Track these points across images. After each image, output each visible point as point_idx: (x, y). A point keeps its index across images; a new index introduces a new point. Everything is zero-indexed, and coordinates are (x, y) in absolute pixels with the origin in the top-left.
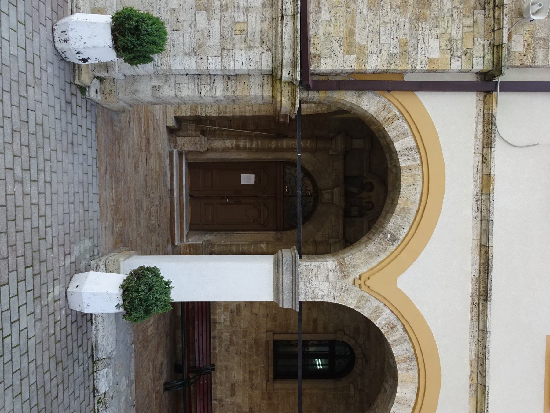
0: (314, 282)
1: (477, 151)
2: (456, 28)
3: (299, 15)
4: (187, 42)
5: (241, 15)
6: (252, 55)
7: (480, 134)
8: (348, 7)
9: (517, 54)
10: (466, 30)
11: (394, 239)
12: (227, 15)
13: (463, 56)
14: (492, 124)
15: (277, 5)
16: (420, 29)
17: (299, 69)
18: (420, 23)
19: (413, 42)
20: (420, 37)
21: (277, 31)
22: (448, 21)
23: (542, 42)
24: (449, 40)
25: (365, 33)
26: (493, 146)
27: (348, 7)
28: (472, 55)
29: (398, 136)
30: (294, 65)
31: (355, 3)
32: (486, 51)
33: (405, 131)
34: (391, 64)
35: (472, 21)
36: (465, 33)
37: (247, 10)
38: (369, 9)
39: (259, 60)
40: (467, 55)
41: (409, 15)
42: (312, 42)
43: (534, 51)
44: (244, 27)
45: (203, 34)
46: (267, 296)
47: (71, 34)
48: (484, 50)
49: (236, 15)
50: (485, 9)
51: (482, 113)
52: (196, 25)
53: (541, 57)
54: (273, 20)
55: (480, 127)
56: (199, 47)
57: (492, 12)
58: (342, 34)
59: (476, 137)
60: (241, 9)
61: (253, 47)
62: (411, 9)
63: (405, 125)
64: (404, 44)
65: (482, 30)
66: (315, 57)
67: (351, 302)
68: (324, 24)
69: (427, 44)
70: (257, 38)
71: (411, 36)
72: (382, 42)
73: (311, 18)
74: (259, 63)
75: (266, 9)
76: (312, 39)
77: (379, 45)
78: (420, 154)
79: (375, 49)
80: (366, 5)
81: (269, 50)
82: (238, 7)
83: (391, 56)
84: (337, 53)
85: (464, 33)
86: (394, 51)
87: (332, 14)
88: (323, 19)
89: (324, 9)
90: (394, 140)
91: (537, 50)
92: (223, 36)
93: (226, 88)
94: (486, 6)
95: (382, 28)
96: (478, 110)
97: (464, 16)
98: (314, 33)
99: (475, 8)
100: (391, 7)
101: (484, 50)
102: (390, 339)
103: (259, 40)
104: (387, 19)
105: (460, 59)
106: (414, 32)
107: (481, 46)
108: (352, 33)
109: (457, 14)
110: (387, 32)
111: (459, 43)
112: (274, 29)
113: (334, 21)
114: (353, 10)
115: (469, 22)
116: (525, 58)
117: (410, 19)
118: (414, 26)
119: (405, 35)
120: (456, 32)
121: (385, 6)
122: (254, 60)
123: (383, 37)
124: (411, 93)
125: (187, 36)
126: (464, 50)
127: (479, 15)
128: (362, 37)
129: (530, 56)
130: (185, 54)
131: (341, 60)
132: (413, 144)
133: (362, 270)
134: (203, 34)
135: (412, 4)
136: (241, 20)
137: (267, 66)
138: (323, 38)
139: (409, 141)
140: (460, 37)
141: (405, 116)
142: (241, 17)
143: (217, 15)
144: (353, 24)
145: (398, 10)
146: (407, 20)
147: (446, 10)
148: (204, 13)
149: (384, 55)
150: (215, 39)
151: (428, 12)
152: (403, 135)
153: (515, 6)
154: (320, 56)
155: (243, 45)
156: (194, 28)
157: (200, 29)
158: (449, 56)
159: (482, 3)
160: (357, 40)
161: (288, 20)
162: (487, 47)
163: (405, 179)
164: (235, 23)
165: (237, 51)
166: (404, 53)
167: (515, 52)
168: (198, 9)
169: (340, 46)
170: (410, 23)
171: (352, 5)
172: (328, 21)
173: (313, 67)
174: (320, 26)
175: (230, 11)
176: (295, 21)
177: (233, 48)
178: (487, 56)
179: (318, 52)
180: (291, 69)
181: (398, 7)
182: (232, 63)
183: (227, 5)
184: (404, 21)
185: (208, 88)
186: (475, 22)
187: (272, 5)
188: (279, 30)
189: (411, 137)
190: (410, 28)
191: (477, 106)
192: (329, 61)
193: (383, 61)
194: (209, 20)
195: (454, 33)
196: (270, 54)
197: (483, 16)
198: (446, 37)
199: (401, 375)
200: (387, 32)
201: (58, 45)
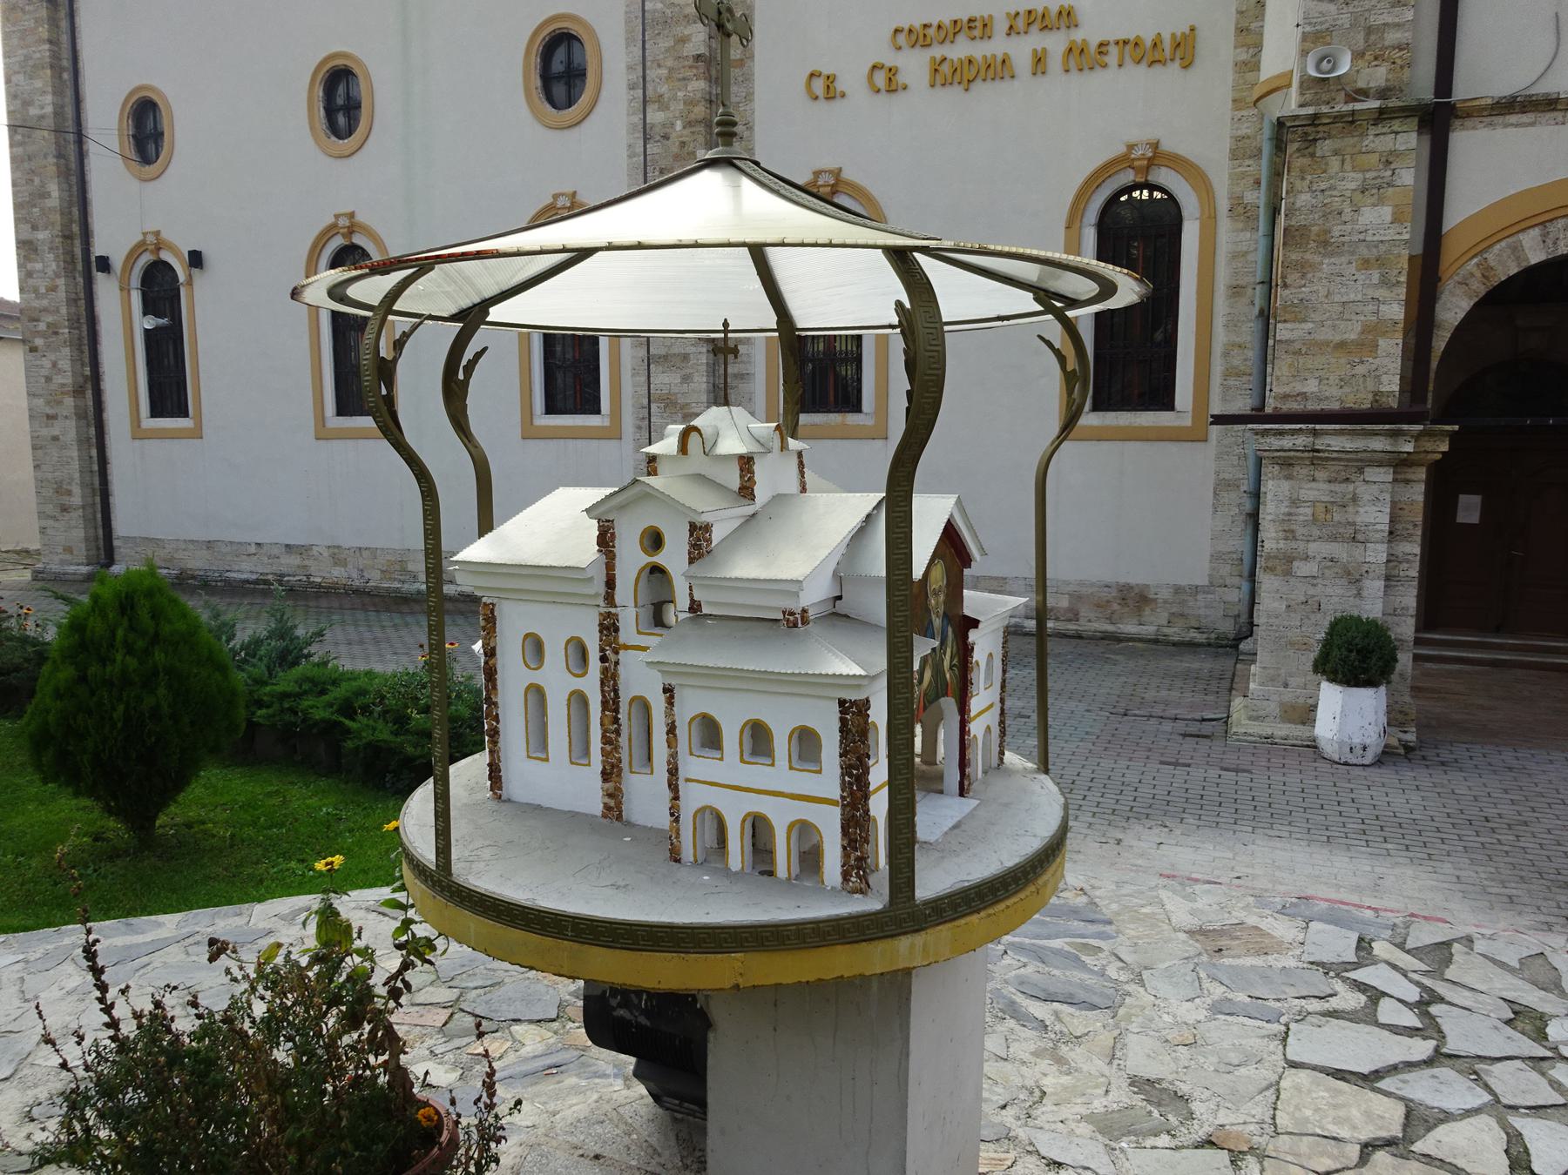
1: (1560, 119)
2: (1343, 183)
3: (1318, 427)
4: (1340, 591)
5: (1301, 510)
6: (1367, 497)
7: (1526, 118)
8: (1299, 353)
9: (1390, 76)
10: (1348, 166)
12: (1300, 531)
13: (1393, 166)
14: (1515, 101)
15: (1289, 458)
16: (1342, 239)
17: (1405, 427)
18: (1333, 240)
19: (1363, 251)
20: (1355, 238)
21: (1334, 459)
22: (1331, 196)
23: (1373, 37)
24: (1363, 192)
25: (1342, 325)
26: (1555, 96)
27: (1299, 353)
28: (1391, 152)
29: (1518, 258)
31: (1293, 341)
32: (1384, 130)
33: (1509, 246)
34: (1398, 282)
35: (1334, 158)
36: (1353, 167)
37: (1295, 502)
38: (1304, 321)
39: (1376, 486)
40: (1390, 160)
41: (1317, 259)
42: (1352, 405)
43: (1386, 48)
44: (1320, 508)
45: (1327, 568)
47: (1357, 740)
48: (1384, 134)
49: (1301, 518)
50: (1315, 140)
51: (1488, 120)
52: (1314, 577)
53: (1398, 35)
54: (1313, 464)
55: (1513, 119)
56: (1349, 574)
57: (1320, 128)
58: (1343, 361)
59: (1532, 124)
60: (1292, 511)
61: (1355, 494)
62: (1308, 256)
63: (1498, 246)
64: (1366, 264)
65: (1350, 141)
66: (1377, 401)
68: (1325, 388)
69: (1368, 227)
71: (1353, 253)
72: (1359, 297)
73: (1312, 406)
74: (1382, 486)
75: (1295, 474)
76: (1348, 405)
77: (1364, 302)
78: (1556, 218)
79: (1371, 308)
80: (1297, 325)
81: (1361, 470)
82: (1290, 514)
83: (1385, 282)
84: (1374, 367)
85: (1354, 169)
86: (1376, 276)
87: (1307, 374)
88: (1316, 390)
89: (1299, 387)
90: (1524, 265)
91: (1387, 43)
92: (1334, 538)
93: (1408, 538)
94: (1311, 138)
95: (1337, 298)
96: (1482, 125)
97: (1325, 172)
98: (1338, 403)
99: (1313, 155)
100: (1304, 286)
101: (1384, 134)
103: (1344, 485)
104: (1323, 292)
105: (1397, 172)
106: (1346, 248)
107: (1377, 140)
108: (1342, 345)
109: (1320, 184)
110: (1342, 290)
111: (1368, 175)
112: (1329, 463)
113: (1321, 373)
114: (1304, 344)
115: (1335, 163)
116: (1399, 62)
117: (1324, 256)
118: (1336, 250)
119: (1350, 263)
120: (1352, 181)
121: (1301, 296)
122: (1376, 494)
123: (1352, 297)
124: (1444, 241)
125: (1329, 591)
126: (1381, 167)
127: (1324, 147)
128: (1350, 328)
129: (1396, 54)
130: (1359, 595)
131: (1386, 361)
132: (1536, 232)
134: (1327, 568)
135: (1301, 255)
136: (1309, 511)
137: (1384, 475)
138: (1347, 389)
140: (1360, 175)
141: (1481, 248)
142: (1305, 512)
143: (1301, 546)
144: (1327, 343)
145: (1310, 276)
146: (1326, 261)
147: (1314, 201)
148: (1296, 564)
149: (1381, 293)
150: (1339, 550)
151: (1315, 229)
152: (1516, 250)
153: (1309, 89)
154: (1376, 394)
155: (1350, 509)
156: (1319, 581)
157: (1320, 572)
158: (1390, 189)
159: (1307, 144)
160: (1353, 336)
161: (1320, 443)
162: (1379, 129)
164: (1315, 519)
165: (1359, 520)
166: (1380, 262)
167: (1387, 80)
168: (1288, 573)
169: (1362, 362)
170: (1332, 255)
171: (1297, 346)
172: (1320, 381)
174: (1327, 394)
175: (1294, 527)
176: (1326, 433)
177: (1354, 524)
178: (1395, 128)
179: (1370, 396)
180: (1401, 440)
181: (1303, 276)
182: (1378, 527)
183: (1285, 531)
184: (1327, 265)
185: (1405, 565)
186: (1336, 153)
187: (1290, 465)
188: (1335, 455)
189: (1521, 236)
190: (1340, 254)
191: (1474, 128)
192: (1385, 379)
193: (1393, 295)
194: (1306, 558)
195: (1353, 185)
196: (1366, 469)
197: (1327, 142)
198: (1358, 197)
200: (1342, 290)
201: (1366, 762)
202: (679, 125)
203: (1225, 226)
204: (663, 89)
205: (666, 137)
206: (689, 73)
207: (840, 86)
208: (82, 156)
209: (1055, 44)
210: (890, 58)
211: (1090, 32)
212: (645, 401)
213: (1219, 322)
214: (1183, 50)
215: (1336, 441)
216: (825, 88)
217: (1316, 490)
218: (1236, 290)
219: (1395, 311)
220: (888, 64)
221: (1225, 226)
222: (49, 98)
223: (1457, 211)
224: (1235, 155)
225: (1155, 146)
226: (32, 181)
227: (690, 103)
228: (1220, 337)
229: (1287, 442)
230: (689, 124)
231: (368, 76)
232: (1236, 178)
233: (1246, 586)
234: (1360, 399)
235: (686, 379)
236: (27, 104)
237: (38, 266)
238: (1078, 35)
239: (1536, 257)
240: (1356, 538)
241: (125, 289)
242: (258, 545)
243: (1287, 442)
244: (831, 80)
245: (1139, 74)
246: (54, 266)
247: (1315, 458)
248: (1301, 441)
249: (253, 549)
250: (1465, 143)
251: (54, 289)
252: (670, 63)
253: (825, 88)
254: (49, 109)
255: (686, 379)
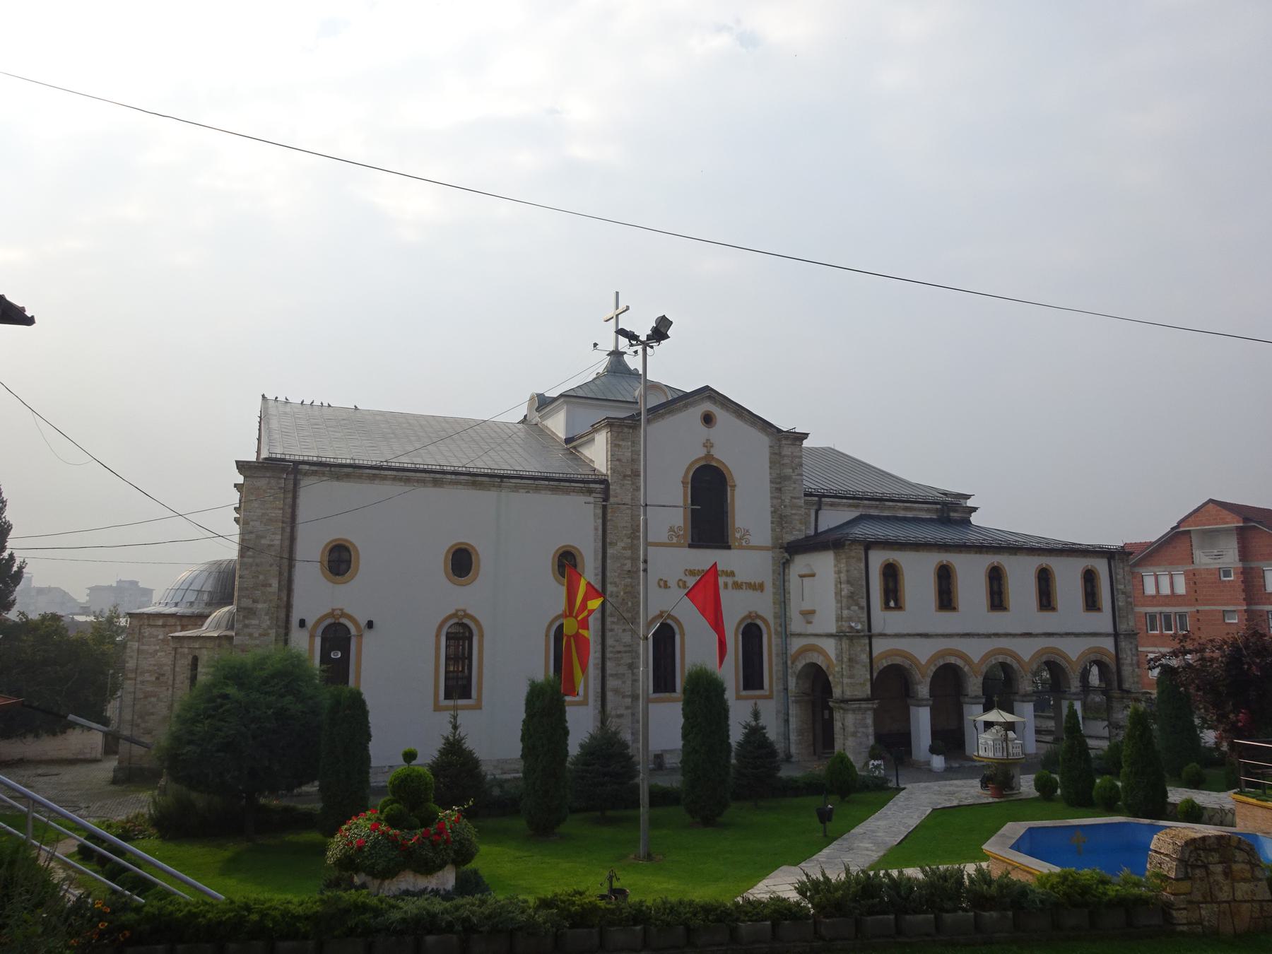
0: (924, 693)
11: (911, 665)
30: (873, 704)
37: (856, 719)
46: (928, 708)
67: (929, 680)
70: (864, 716)
73: (857, 697)
102: (938, 665)
127: (854, 641)
133: (920, 676)
139: (884, 661)
150: (863, 730)
163: (895, 662)
173: (870, 696)
199: (948, 662)
202: (622, 593)
203: (773, 636)
204: (617, 580)
205: (617, 596)
206: (626, 576)
207: (669, 585)
208: (291, 567)
209: (730, 580)
210: (684, 578)
211: (740, 578)
212: (599, 690)
213: (774, 664)
214: (760, 587)
215: (864, 705)
216: (664, 585)
217: (859, 717)
218: (777, 655)
219: (869, 677)
220: (684, 579)
221: (773, 636)
222: (279, 537)
223: (875, 654)
224: (775, 617)
225: (756, 613)
226: (258, 577)
227: (626, 586)
228: (774, 668)
229: (855, 706)
230: (625, 593)
231: (477, 554)
232: (775, 624)
233: (787, 741)
234: (865, 696)
235: (624, 682)
236: (259, 537)
237: (254, 622)
238: (736, 579)
239: (885, 665)
240: (867, 727)
241: (312, 636)
242: (391, 767)
243: (855, 706)
244: (666, 582)
245: (750, 592)
246: (268, 623)
247: (860, 709)
248: (858, 706)
249: (387, 769)
250: (874, 641)
251: (266, 635)
252: (619, 571)
253: (664, 585)
254: (277, 543)
255: (624, 682)
